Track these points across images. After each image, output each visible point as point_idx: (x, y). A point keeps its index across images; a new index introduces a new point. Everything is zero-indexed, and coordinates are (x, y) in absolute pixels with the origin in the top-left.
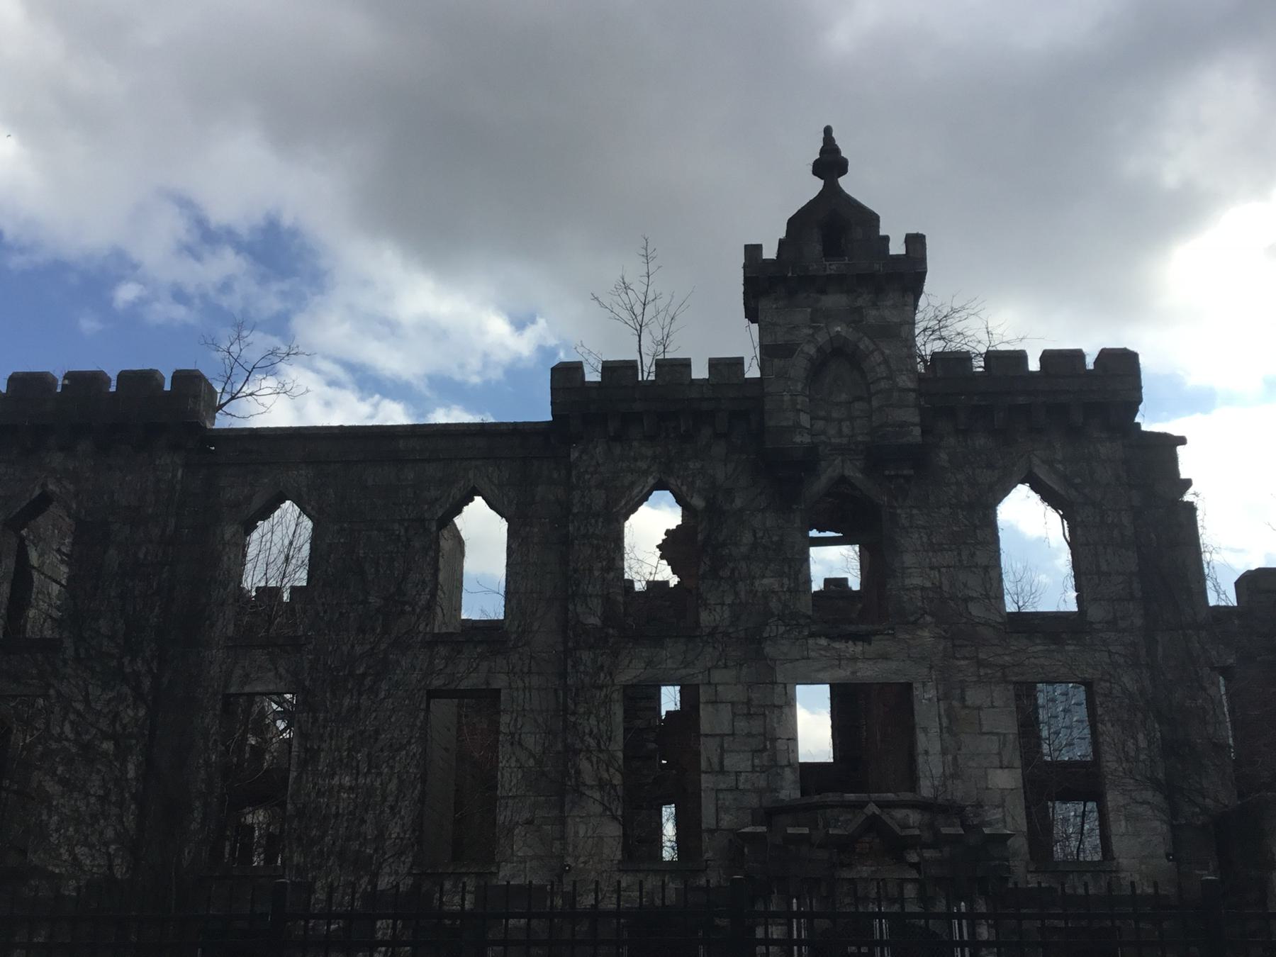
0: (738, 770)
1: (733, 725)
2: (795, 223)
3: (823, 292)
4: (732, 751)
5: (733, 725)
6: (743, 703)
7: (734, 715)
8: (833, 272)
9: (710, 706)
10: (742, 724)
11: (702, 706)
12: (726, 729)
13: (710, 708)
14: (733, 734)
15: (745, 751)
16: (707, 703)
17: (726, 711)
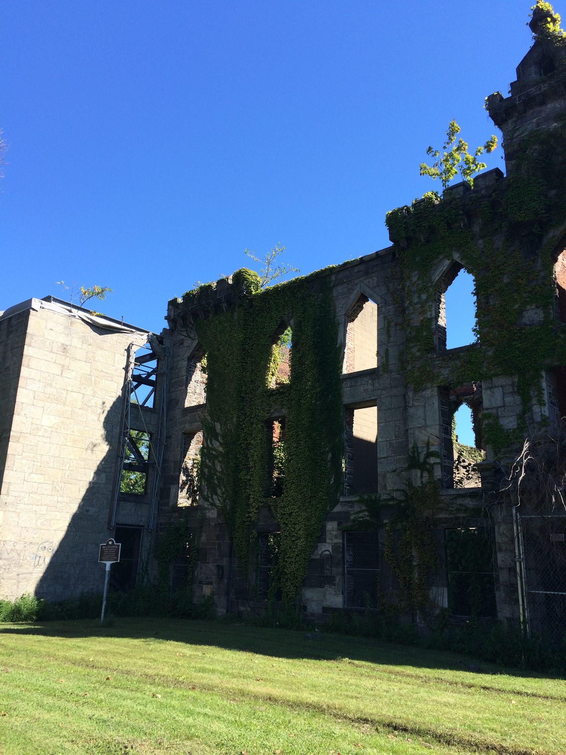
0: (508, 428)
1: (504, 400)
2: (522, 69)
3: (543, 103)
4: (504, 417)
5: (504, 400)
6: (509, 385)
7: (504, 394)
8: (546, 88)
9: (488, 390)
10: (509, 399)
11: (483, 391)
12: (499, 403)
13: (489, 392)
14: (504, 406)
15: (514, 415)
16: (486, 389)
17: (498, 392)
